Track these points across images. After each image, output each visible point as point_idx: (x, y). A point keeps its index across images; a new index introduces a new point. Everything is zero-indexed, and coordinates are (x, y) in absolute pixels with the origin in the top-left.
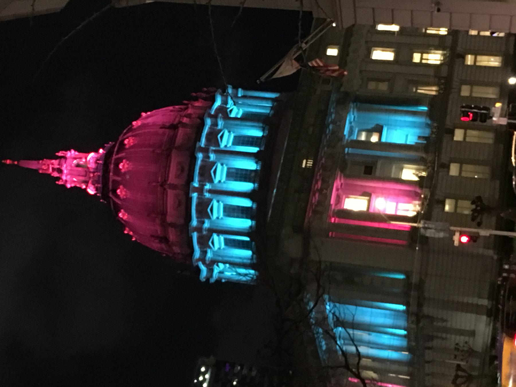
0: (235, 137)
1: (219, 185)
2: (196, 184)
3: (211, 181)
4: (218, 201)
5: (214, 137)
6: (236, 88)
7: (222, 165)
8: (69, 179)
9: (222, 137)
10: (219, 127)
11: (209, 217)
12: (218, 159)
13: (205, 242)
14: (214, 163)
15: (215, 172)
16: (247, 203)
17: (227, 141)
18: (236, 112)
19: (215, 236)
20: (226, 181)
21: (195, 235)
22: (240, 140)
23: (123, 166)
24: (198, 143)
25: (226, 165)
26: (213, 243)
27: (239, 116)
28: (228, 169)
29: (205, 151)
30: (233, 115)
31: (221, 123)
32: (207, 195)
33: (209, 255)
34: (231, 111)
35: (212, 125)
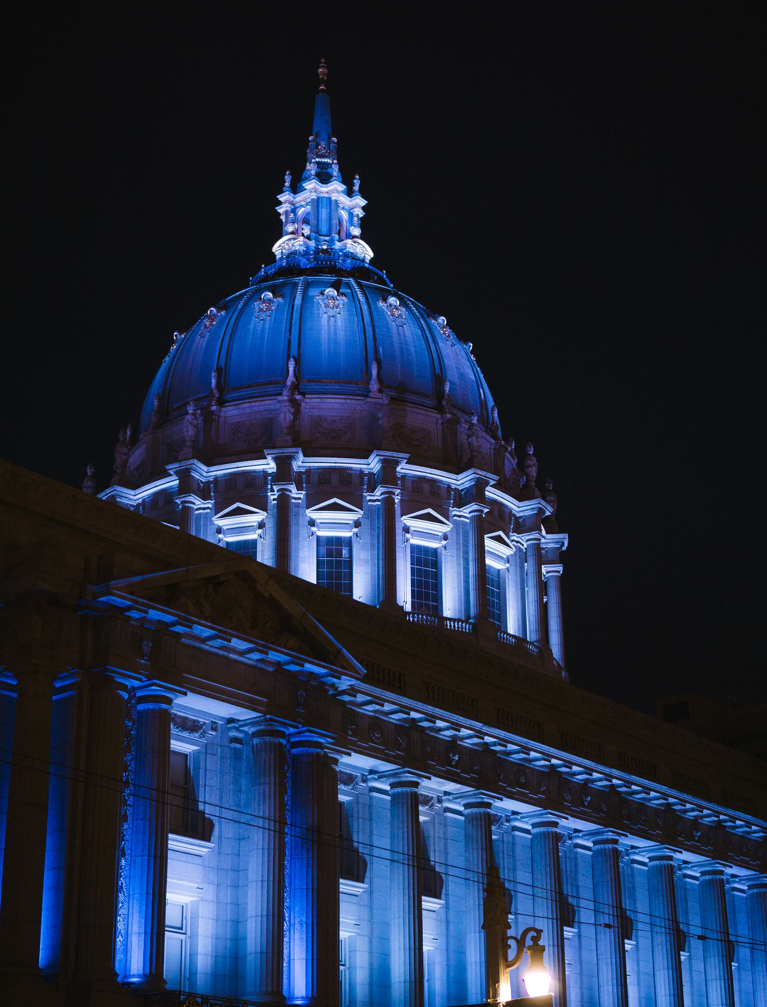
0: (435, 551)
1: (303, 522)
2: (301, 463)
4: (261, 525)
5: (428, 499)
6: (562, 557)
7: (357, 524)
9: (429, 518)
10: (454, 511)
11: (218, 509)
12: (370, 514)
14: (358, 503)
17: (421, 531)
18: (499, 554)
20: (315, 539)
21: (171, 482)
22: (427, 567)
23: (333, 298)
24: (407, 456)
28: (349, 542)
30: (490, 544)
31: (467, 512)
32: (273, 497)
34: (499, 539)
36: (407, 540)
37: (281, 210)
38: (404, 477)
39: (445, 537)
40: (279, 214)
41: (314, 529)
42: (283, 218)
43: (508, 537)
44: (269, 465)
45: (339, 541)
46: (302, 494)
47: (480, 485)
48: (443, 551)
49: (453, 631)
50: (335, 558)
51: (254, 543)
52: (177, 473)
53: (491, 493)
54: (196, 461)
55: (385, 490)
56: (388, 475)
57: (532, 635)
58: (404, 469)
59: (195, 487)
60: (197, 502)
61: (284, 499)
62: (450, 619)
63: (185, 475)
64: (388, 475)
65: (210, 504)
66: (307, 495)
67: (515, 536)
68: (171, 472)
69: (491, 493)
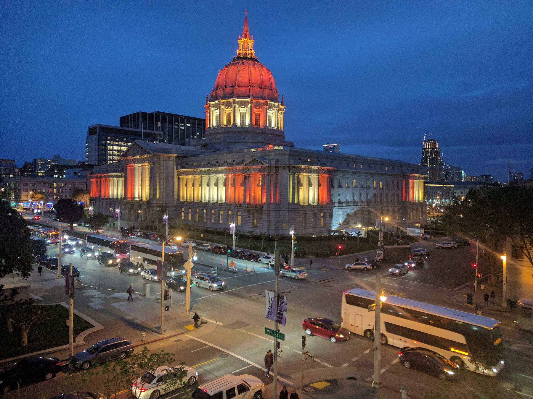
3: (239, 106)
5: (258, 105)
13: (217, 106)
16: (232, 123)
17: (257, 111)
19: (218, 111)
22: (258, 117)
27: (268, 114)
29: (251, 102)
50: (243, 116)
56: (251, 102)
69: (269, 102)
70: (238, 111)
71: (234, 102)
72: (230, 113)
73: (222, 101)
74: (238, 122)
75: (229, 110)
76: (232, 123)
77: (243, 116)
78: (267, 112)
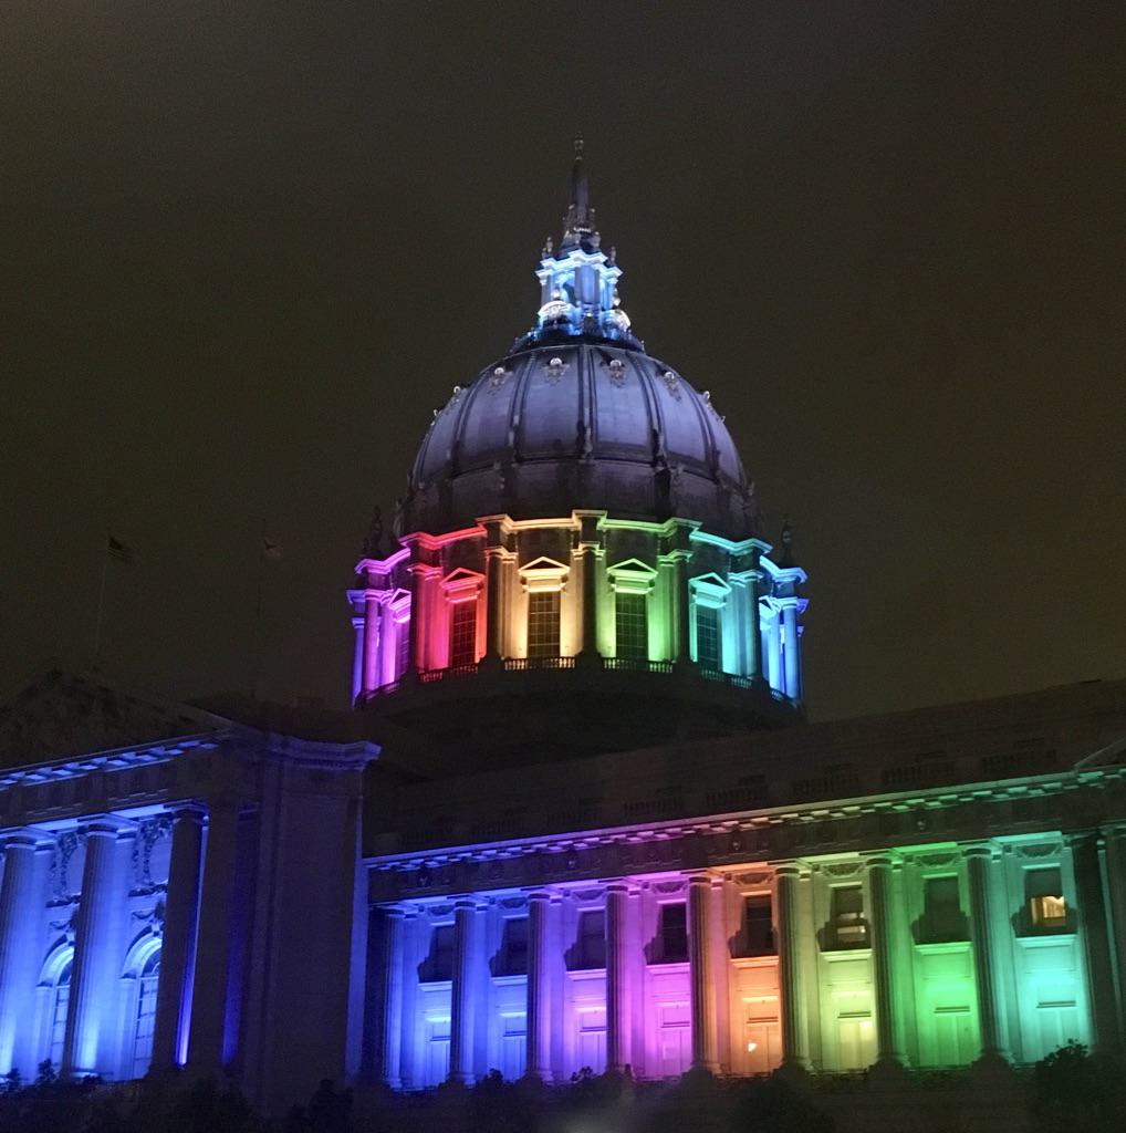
2: (509, 525)
3: (522, 562)
4: (480, 587)
7: (564, 579)
8: (556, 270)
10: (662, 559)
11: (446, 575)
13: (403, 579)
15: (543, 565)
16: (480, 651)
17: (631, 580)
21: (405, 554)
22: (632, 616)
25: (564, 589)
26: (401, 596)
27: (698, 601)
31: (673, 556)
33: (379, 596)
35: (664, 540)
36: (613, 590)
37: (540, 274)
38: (609, 531)
39: (652, 584)
40: (538, 279)
41: (525, 587)
42: (543, 282)
43: (725, 579)
44: (479, 532)
45: (549, 596)
46: (515, 556)
47: (684, 532)
48: (648, 597)
49: (655, 673)
50: (544, 611)
51: (475, 601)
52: (409, 545)
53: (697, 536)
54: (422, 534)
55: (584, 545)
56: (590, 531)
57: (750, 670)
58: (604, 523)
59: (424, 556)
60: (430, 573)
61: (495, 561)
62: (657, 663)
63: (414, 546)
64: (590, 531)
65: (438, 571)
66: (520, 557)
67: (732, 576)
68: (404, 544)
69: (697, 536)
70: (516, 585)
71: (494, 536)
72: (474, 603)
73: (431, 542)
74: (519, 642)
75: (467, 589)
76: (480, 651)
77: (544, 611)
78: (685, 594)
